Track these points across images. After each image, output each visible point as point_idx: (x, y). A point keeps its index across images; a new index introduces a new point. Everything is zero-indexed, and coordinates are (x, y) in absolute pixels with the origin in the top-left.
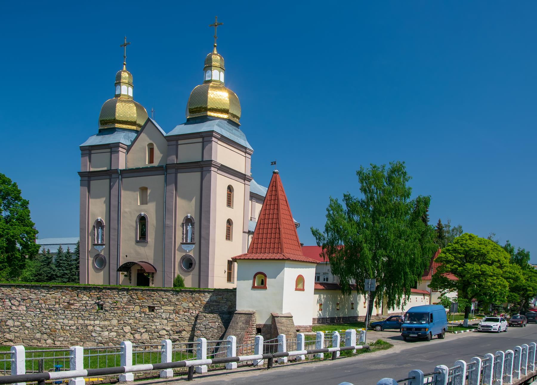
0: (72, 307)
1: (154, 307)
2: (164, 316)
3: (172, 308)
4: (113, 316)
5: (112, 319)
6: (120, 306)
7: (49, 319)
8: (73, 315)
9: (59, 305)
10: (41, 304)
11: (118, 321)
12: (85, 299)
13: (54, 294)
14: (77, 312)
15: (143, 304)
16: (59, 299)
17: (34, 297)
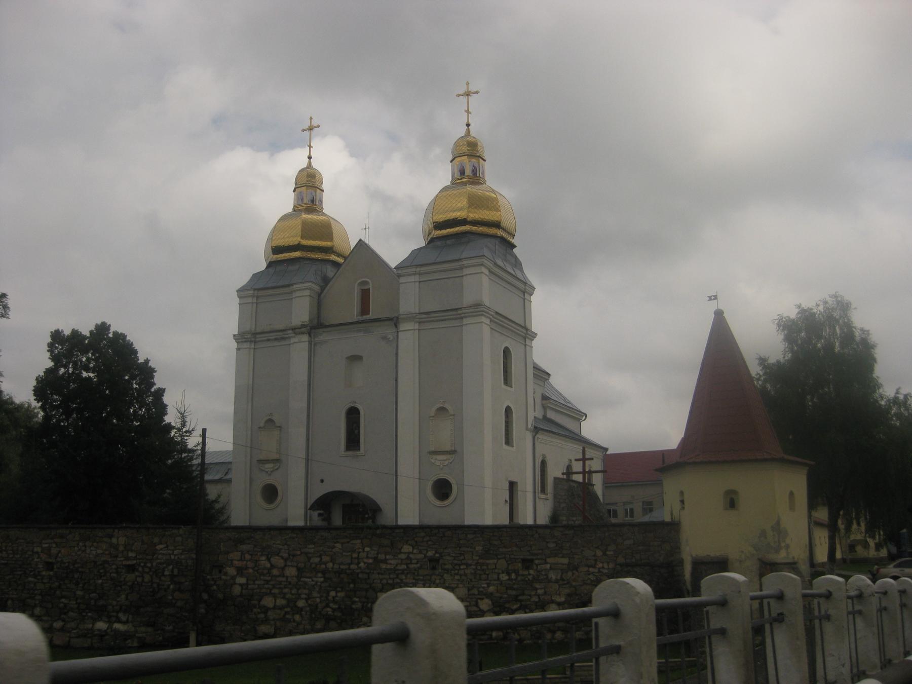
0: (383, 566)
1: (532, 561)
2: (553, 576)
3: (565, 561)
4: (458, 580)
5: (456, 587)
6: (470, 562)
7: (339, 591)
8: (384, 581)
9: (359, 563)
10: (325, 564)
11: (469, 590)
12: (407, 551)
13: (348, 542)
14: (392, 576)
15: (512, 556)
16: (359, 553)
17: (312, 551)
